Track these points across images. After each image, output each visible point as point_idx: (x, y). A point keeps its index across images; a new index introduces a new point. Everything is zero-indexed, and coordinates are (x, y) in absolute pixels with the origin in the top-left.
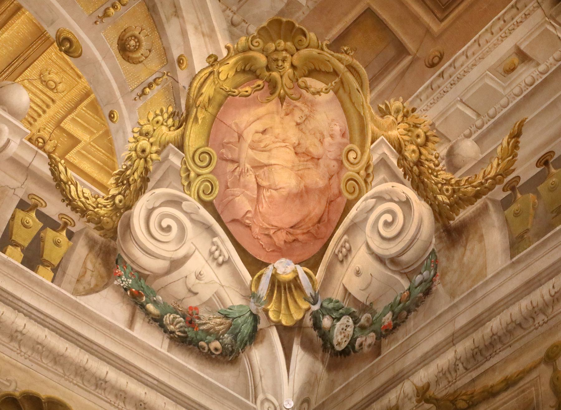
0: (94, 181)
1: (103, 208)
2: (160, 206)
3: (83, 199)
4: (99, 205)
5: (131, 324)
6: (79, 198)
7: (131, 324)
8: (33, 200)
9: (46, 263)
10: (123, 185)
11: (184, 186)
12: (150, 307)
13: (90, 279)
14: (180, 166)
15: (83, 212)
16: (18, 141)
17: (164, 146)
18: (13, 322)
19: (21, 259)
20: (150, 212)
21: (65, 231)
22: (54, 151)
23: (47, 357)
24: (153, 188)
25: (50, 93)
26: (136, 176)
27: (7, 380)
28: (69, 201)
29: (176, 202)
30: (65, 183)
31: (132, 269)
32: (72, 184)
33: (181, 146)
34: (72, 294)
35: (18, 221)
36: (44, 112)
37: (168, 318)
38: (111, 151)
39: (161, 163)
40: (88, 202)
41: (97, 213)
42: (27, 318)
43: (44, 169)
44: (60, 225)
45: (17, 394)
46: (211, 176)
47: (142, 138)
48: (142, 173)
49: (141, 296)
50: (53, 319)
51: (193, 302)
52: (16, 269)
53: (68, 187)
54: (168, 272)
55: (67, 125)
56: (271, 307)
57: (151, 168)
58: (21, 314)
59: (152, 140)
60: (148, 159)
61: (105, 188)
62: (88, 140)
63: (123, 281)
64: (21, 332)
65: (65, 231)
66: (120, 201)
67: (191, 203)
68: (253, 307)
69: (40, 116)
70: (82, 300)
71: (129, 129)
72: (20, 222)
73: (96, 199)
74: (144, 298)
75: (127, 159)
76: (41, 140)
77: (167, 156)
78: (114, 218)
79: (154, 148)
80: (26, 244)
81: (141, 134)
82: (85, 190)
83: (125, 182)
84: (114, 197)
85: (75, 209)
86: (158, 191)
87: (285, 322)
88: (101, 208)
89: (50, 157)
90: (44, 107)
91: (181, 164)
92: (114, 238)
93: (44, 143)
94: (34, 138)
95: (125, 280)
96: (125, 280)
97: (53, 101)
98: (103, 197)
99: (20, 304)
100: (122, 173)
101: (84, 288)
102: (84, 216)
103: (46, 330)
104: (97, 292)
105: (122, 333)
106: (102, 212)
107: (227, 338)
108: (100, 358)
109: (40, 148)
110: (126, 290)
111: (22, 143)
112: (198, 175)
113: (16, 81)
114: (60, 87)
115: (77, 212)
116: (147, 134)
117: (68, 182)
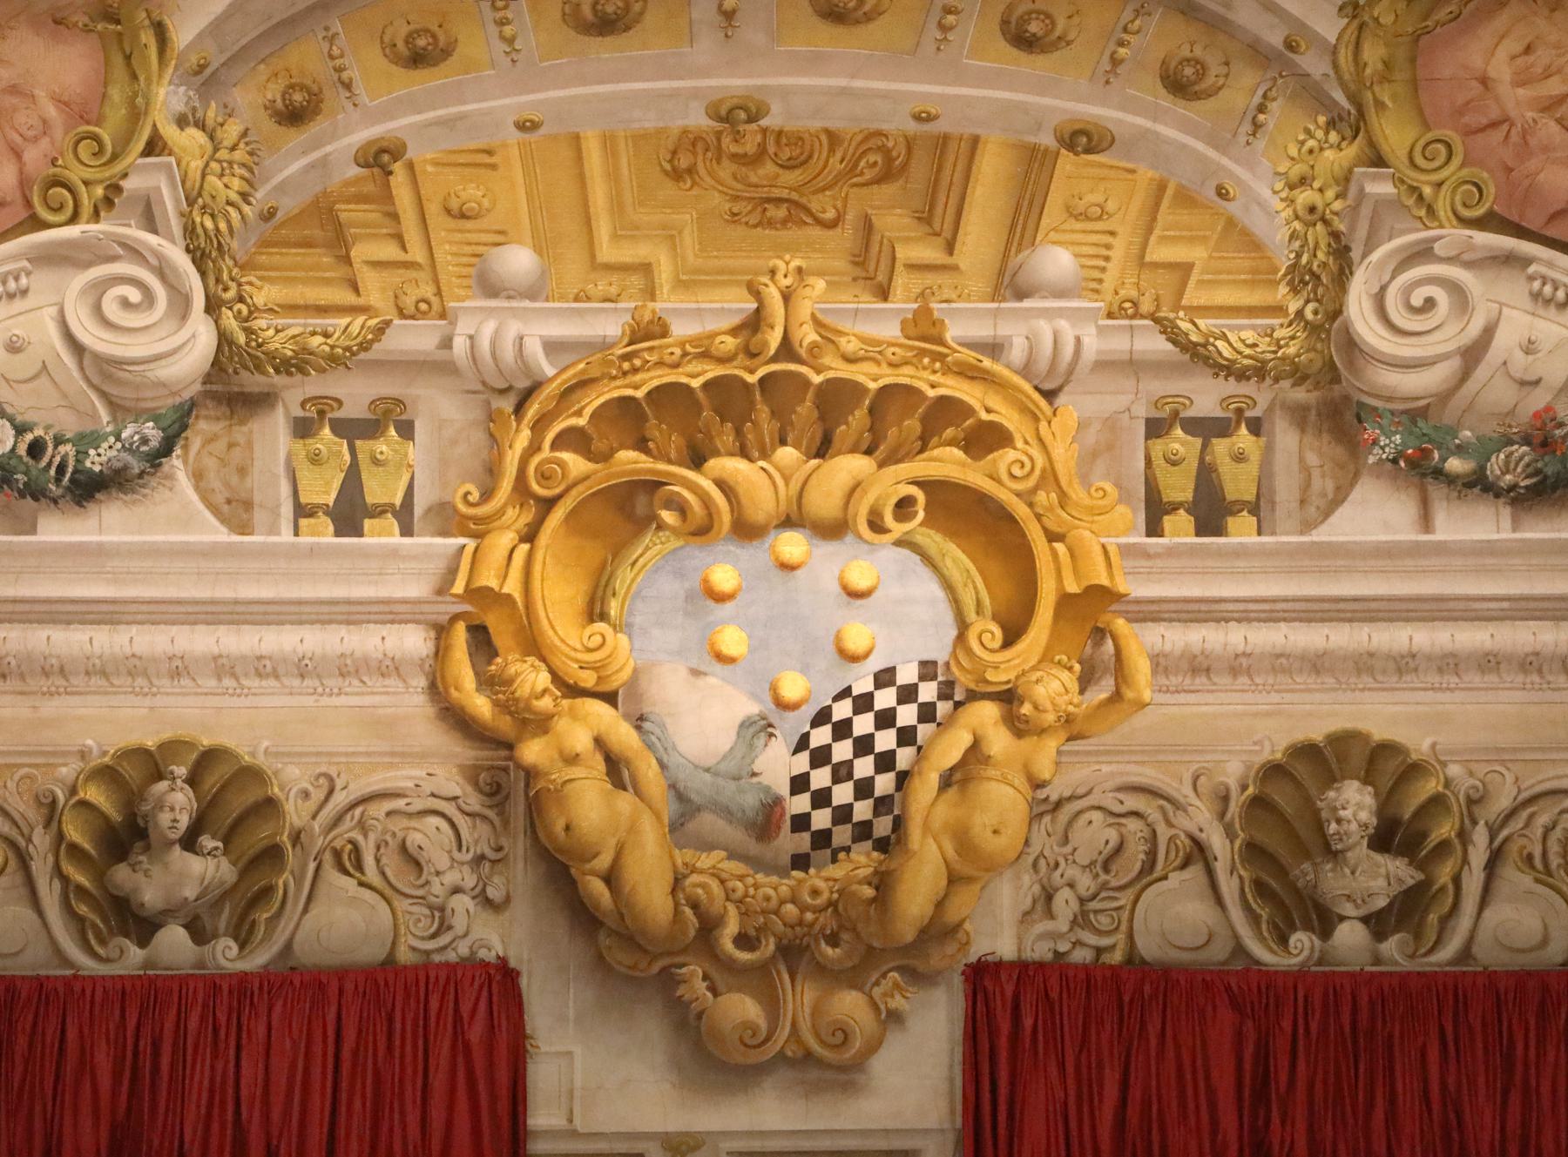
0: (1251, 311)
1: (1292, 343)
2: (1393, 278)
3: (1248, 351)
4: (1282, 342)
5: (1426, 521)
6: (1240, 353)
7: (1426, 521)
8: (1167, 407)
9: (1233, 509)
10: (1307, 284)
11: (1420, 218)
12: (1455, 465)
13: (1323, 484)
14: (1396, 191)
15: (1259, 372)
16: (1092, 330)
17: (1345, 180)
18: (1226, 645)
19: (1191, 527)
20: (1379, 300)
21: (1243, 425)
22: (1158, 308)
23: (1301, 670)
24: (1365, 256)
25: (1099, 226)
26: (1321, 255)
27: (1255, 743)
28: (1227, 370)
30: (1204, 346)
31: (1392, 413)
32: (1216, 339)
33: (1379, 161)
34: (1302, 533)
35: (1158, 461)
36: (1107, 259)
38: (1253, 244)
39: (1355, 208)
40: (1258, 350)
41: (1283, 359)
42: (1244, 624)
43: (1155, 344)
44: (1229, 419)
45: (1279, 756)
46: (1465, 172)
47: (1298, 190)
48: (1329, 245)
49: (1425, 454)
50: (1286, 600)
51: (1538, 400)
52: (1192, 551)
53: (1211, 348)
54: (1465, 375)
55: (1160, 253)
57: (1342, 227)
58: (1231, 623)
59: (1316, 185)
60: (1328, 217)
61: (1278, 310)
62: (1205, 255)
63: (1382, 448)
64: (1244, 654)
65: (1243, 425)
66: (1316, 313)
67: (1452, 236)
69: (1100, 281)
70: (1321, 535)
71: (1266, 193)
72: (1162, 461)
73: (1271, 336)
74: (1436, 455)
75: (1290, 241)
76: (1127, 305)
77: (1362, 190)
78: (1319, 346)
79: (1330, 194)
80: (1188, 495)
81: (1292, 187)
82: (1244, 335)
83: (1307, 277)
84: (1300, 313)
85: (1242, 375)
86: (1375, 256)
88: (1287, 345)
89: (1156, 320)
90: (1104, 252)
91: (1395, 186)
92: (1336, 379)
93: (1135, 304)
94: (1115, 308)
95: (1387, 441)
96: (1387, 441)
97: (1112, 233)
98: (1282, 325)
99: (1223, 606)
100: (1292, 268)
101: (1318, 508)
102: (1264, 379)
103: (1282, 625)
104: (1343, 501)
105: (1415, 550)
106: (1292, 350)
108: (1391, 620)
109: (1132, 317)
110: (1395, 461)
111: (1101, 330)
112: (1440, 185)
113: (1037, 241)
114: (1111, 206)
115: (1248, 379)
116: (1303, 181)
117: (1208, 341)
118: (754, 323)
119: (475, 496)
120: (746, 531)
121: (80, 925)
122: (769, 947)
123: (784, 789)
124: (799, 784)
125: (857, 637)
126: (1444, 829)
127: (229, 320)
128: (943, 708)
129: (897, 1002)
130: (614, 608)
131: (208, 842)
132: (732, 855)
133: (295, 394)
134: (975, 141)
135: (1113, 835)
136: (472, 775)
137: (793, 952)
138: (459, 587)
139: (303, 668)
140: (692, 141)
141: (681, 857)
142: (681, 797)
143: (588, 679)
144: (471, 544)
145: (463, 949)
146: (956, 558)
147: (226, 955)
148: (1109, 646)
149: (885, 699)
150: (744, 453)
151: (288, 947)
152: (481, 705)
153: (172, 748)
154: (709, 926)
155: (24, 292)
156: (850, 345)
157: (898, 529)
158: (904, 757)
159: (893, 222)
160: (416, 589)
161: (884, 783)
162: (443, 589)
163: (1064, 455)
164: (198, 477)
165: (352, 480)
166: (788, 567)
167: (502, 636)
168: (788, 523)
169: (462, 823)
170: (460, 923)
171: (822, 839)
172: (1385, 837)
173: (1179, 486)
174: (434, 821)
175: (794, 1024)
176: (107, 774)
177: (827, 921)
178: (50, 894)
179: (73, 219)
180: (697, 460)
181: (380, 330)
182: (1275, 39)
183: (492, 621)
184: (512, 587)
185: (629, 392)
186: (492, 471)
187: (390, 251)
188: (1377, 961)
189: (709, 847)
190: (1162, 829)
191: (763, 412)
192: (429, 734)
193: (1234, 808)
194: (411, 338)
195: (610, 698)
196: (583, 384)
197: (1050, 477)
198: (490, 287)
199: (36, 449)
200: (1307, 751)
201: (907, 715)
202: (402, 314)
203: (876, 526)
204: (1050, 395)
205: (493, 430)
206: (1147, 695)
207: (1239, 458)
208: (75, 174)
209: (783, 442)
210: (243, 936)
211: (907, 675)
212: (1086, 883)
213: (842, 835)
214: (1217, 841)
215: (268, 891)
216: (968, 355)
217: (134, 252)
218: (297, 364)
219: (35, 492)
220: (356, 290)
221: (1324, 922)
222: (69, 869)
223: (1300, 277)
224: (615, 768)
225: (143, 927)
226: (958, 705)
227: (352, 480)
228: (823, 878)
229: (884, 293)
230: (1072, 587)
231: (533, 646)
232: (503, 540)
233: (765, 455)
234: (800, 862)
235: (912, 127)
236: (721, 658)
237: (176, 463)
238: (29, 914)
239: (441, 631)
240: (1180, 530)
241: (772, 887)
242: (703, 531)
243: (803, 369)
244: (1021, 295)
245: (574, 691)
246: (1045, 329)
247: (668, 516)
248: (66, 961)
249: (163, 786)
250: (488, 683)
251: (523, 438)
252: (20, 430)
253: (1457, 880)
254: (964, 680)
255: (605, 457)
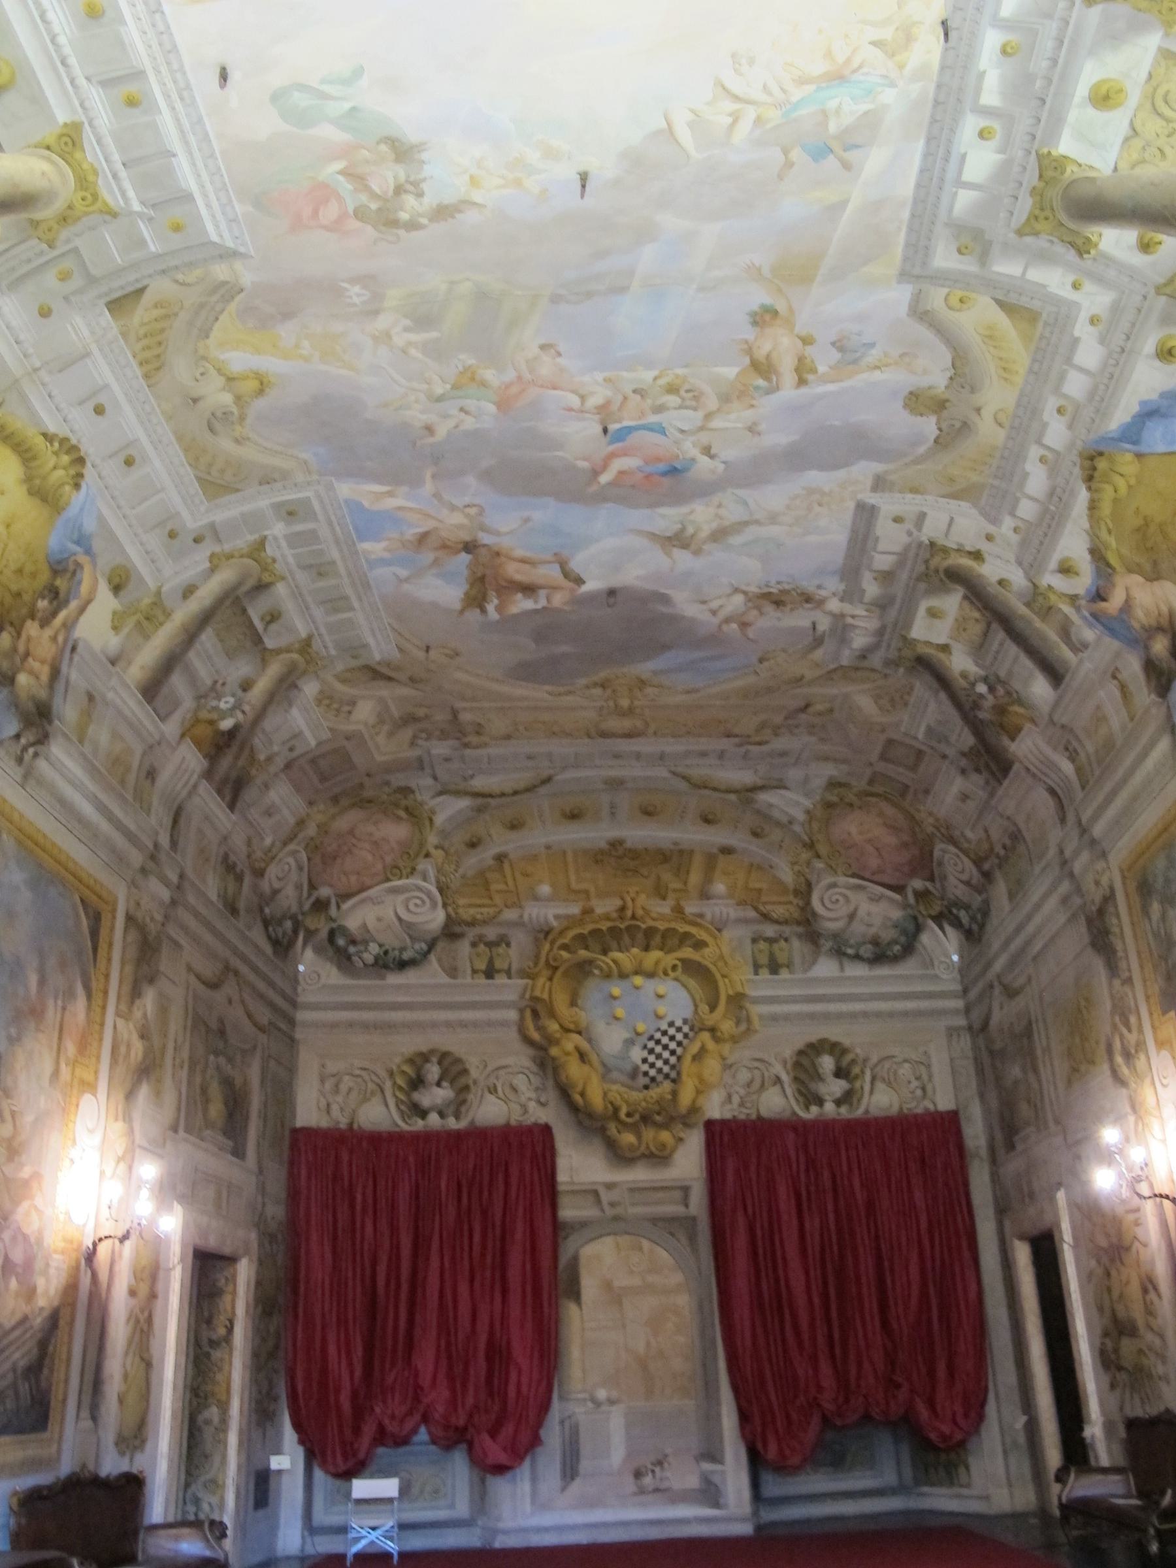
0: (780, 903)
5: (842, 969)
7: (842, 969)
12: (850, 951)
15: (786, 922)
29: (834, 885)
37: (862, 952)
43: (752, 914)
51: (873, 931)
56: (922, 908)
61: (791, 903)
67: (842, 880)
68: (910, 911)
87: (933, 913)
107: (903, 939)
118: (623, 909)
119: (531, 965)
120: (623, 976)
121: (402, 1113)
122: (637, 1117)
123: (639, 1062)
124: (645, 1061)
125: (662, 1010)
126: (856, 1070)
127: (450, 909)
128: (691, 1034)
129: (682, 1135)
130: (579, 1002)
131: (445, 1084)
132: (623, 1085)
133: (472, 933)
134: (692, 852)
135: (749, 1075)
136: (534, 1059)
137: (646, 1119)
138: (527, 996)
139: (475, 1024)
140: (602, 852)
141: (606, 1086)
142: (604, 1065)
143: (572, 1026)
144: (530, 982)
145: (533, 1120)
146: (692, 983)
147: (452, 1123)
148: (745, 1012)
149: (672, 1031)
150: (620, 950)
151: (473, 1120)
152: (536, 1036)
153: (432, 1052)
154: (616, 1110)
155: (383, 902)
156: (654, 915)
157: (672, 974)
158: (679, 1051)
159: (667, 877)
160: (511, 996)
161: (673, 1060)
162: (522, 996)
163: (726, 950)
164: (439, 960)
165: (491, 962)
166: (637, 988)
167: (542, 1013)
168: (636, 973)
169: (531, 1076)
170: (531, 1110)
171: (653, 1079)
172: (839, 1073)
173: (764, 960)
174: (520, 1076)
175: (647, 1144)
176: (411, 1061)
177: (657, 1108)
178: (392, 1102)
179: (400, 878)
180: (605, 952)
181: (500, 912)
182: (784, 819)
183: (539, 1007)
184: (545, 996)
185: (582, 931)
186: (537, 957)
187: (502, 887)
188: (839, 1114)
189: (614, 1082)
190: (766, 1074)
191: (626, 939)
192: (517, 1044)
193: (789, 1066)
194: (510, 915)
195: (580, 1033)
196: (567, 928)
197: (722, 957)
198: (536, 898)
199: (386, 953)
200: (811, 1046)
201: (679, 1037)
202: (507, 906)
203: (666, 974)
204: (719, 930)
205: (537, 943)
206: (758, 1028)
207: (781, 950)
208: (401, 864)
209: (633, 946)
210: (457, 1117)
211: (679, 1023)
212: (742, 1092)
213: (660, 1078)
214: (785, 1077)
215: (464, 1102)
216: (691, 918)
217: (419, 889)
218: (472, 923)
219: (386, 967)
220: (491, 898)
221: (820, 1102)
222: (398, 1094)
223: (796, 893)
224: (583, 1057)
225: (423, 1114)
226: (696, 1033)
227: (491, 962)
228: (654, 1093)
229: (664, 898)
230: (731, 992)
231: (552, 1014)
232: (541, 981)
233: (628, 950)
234: (646, 1087)
235: (672, 847)
236: (617, 1019)
237: (432, 957)
238: (383, 1109)
239: (522, 1011)
240: (765, 974)
241: (636, 1096)
242: (608, 976)
243: (638, 923)
244: (708, 898)
245: (568, 1031)
246: (717, 910)
247: (596, 972)
248: (397, 1125)
249: (428, 1066)
250: (539, 1028)
251: (547, 946)
252: (381, 946)
253: (862, 1088)
254: (697, 1025)
255: (574, 952)
